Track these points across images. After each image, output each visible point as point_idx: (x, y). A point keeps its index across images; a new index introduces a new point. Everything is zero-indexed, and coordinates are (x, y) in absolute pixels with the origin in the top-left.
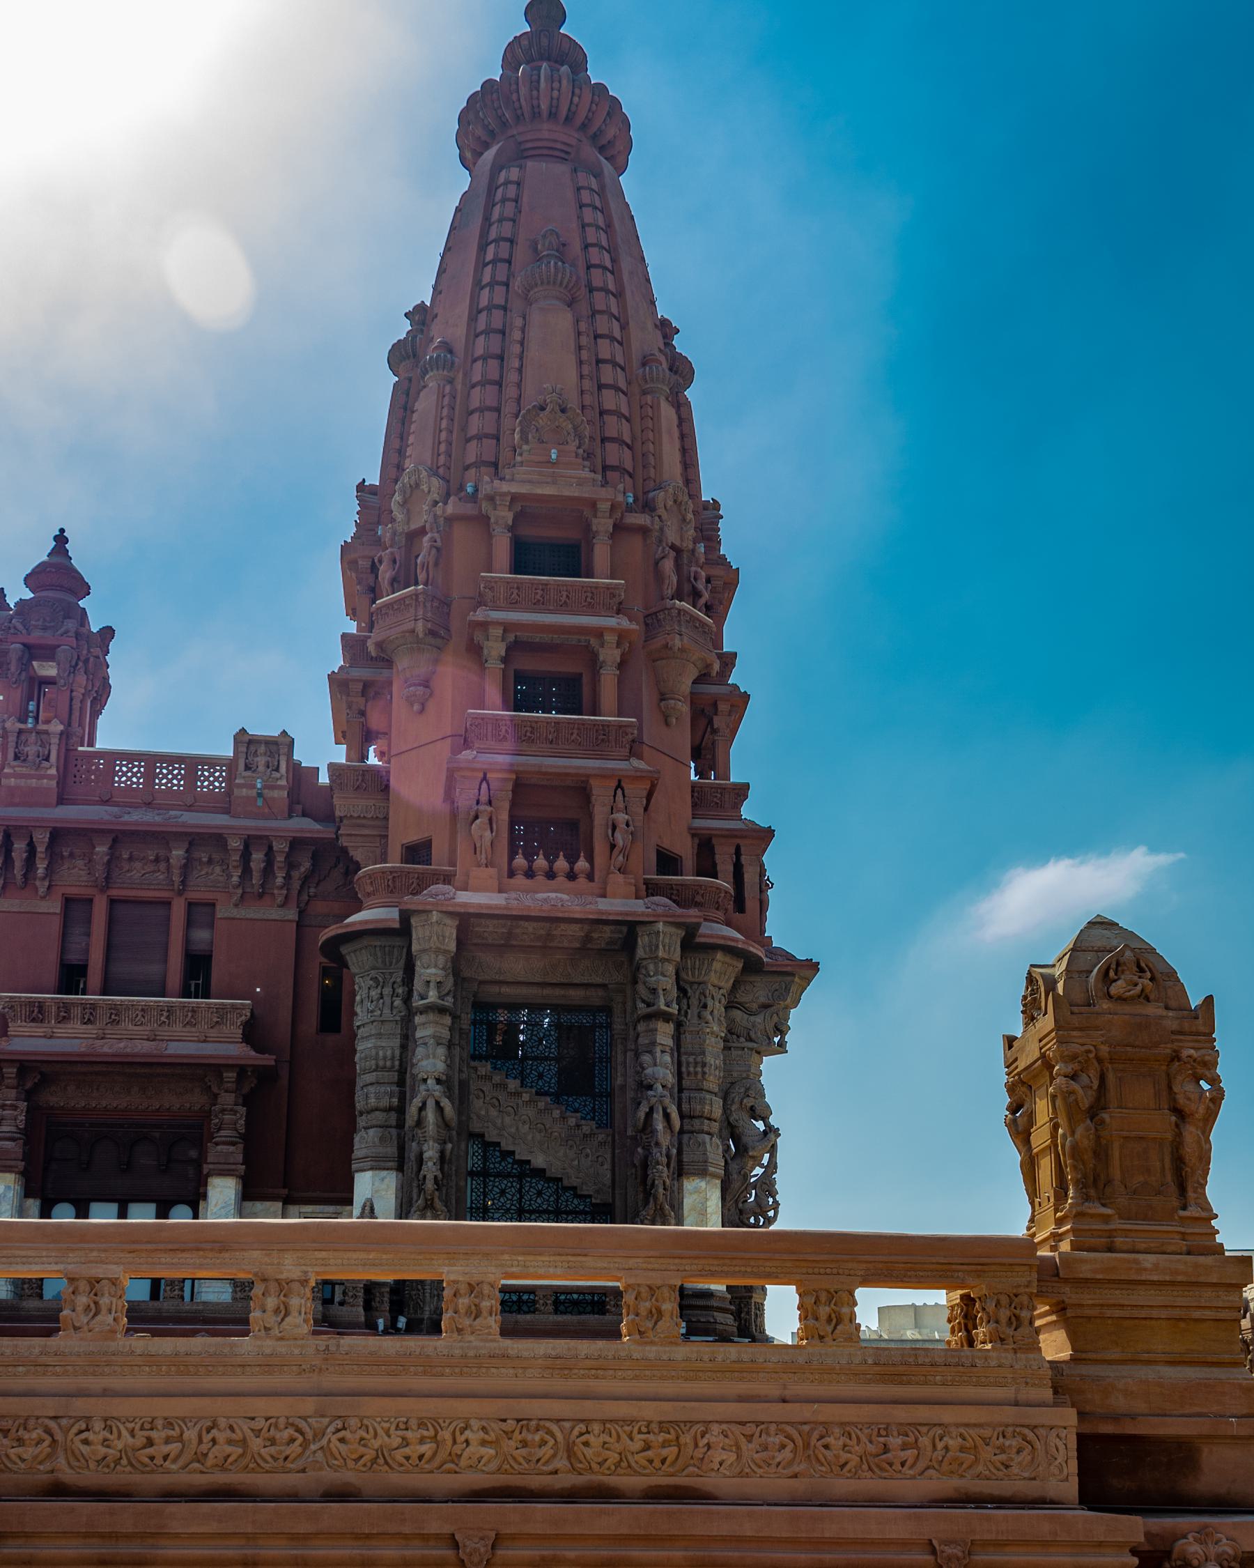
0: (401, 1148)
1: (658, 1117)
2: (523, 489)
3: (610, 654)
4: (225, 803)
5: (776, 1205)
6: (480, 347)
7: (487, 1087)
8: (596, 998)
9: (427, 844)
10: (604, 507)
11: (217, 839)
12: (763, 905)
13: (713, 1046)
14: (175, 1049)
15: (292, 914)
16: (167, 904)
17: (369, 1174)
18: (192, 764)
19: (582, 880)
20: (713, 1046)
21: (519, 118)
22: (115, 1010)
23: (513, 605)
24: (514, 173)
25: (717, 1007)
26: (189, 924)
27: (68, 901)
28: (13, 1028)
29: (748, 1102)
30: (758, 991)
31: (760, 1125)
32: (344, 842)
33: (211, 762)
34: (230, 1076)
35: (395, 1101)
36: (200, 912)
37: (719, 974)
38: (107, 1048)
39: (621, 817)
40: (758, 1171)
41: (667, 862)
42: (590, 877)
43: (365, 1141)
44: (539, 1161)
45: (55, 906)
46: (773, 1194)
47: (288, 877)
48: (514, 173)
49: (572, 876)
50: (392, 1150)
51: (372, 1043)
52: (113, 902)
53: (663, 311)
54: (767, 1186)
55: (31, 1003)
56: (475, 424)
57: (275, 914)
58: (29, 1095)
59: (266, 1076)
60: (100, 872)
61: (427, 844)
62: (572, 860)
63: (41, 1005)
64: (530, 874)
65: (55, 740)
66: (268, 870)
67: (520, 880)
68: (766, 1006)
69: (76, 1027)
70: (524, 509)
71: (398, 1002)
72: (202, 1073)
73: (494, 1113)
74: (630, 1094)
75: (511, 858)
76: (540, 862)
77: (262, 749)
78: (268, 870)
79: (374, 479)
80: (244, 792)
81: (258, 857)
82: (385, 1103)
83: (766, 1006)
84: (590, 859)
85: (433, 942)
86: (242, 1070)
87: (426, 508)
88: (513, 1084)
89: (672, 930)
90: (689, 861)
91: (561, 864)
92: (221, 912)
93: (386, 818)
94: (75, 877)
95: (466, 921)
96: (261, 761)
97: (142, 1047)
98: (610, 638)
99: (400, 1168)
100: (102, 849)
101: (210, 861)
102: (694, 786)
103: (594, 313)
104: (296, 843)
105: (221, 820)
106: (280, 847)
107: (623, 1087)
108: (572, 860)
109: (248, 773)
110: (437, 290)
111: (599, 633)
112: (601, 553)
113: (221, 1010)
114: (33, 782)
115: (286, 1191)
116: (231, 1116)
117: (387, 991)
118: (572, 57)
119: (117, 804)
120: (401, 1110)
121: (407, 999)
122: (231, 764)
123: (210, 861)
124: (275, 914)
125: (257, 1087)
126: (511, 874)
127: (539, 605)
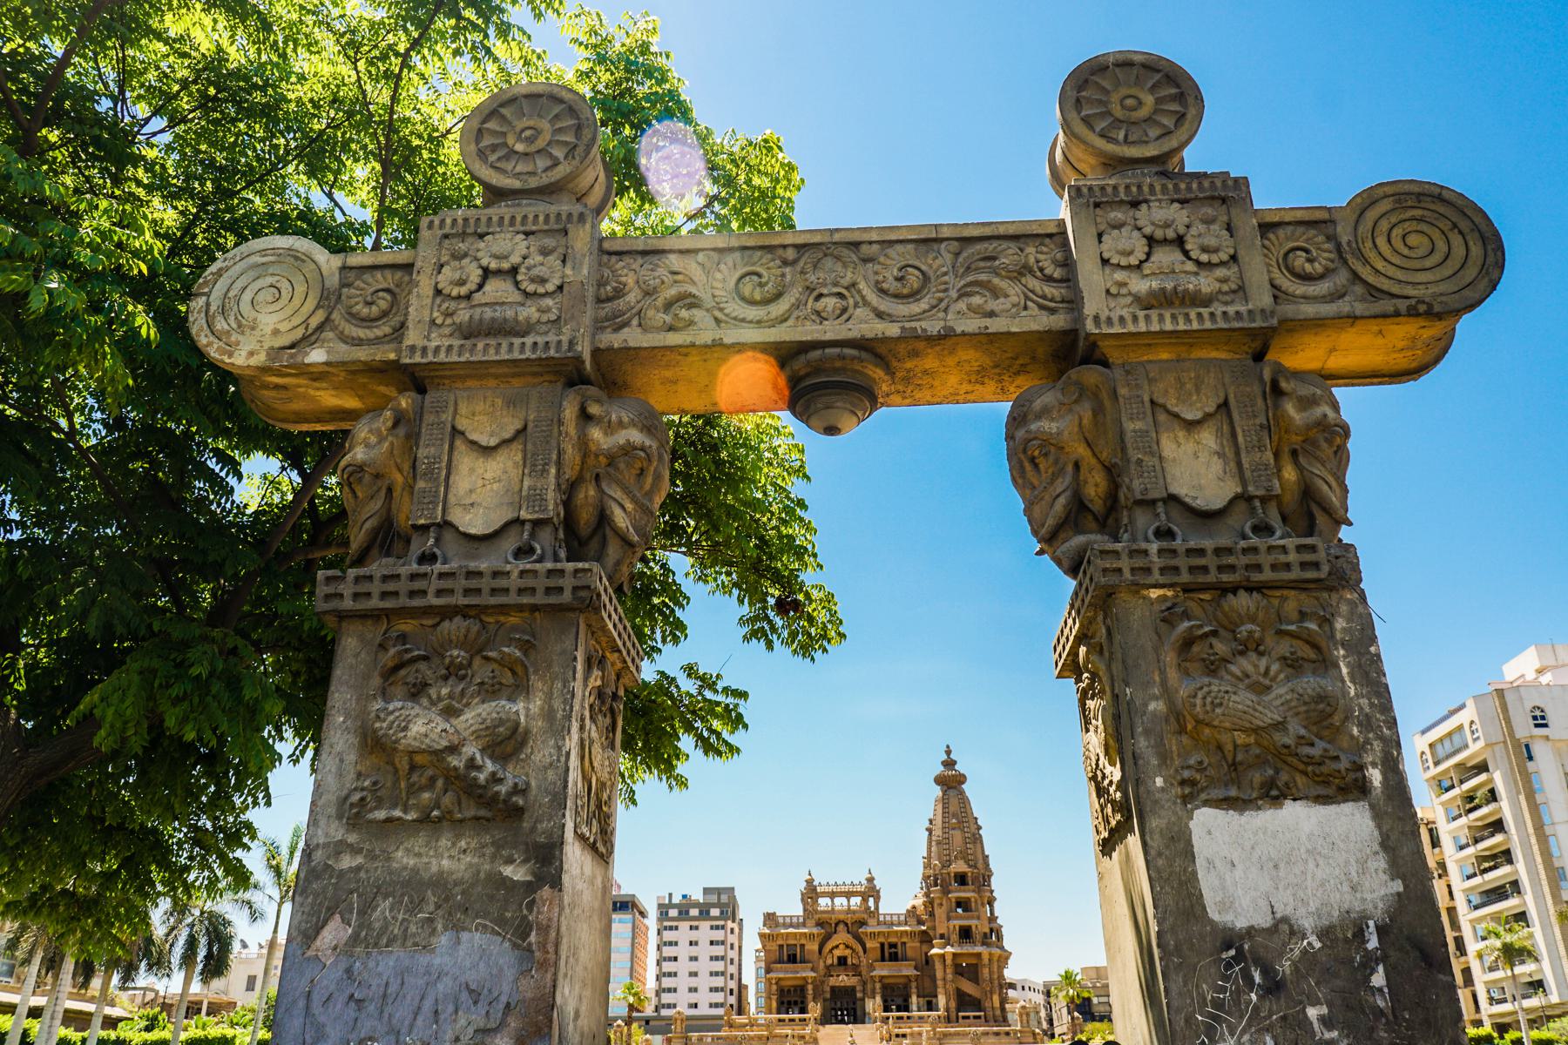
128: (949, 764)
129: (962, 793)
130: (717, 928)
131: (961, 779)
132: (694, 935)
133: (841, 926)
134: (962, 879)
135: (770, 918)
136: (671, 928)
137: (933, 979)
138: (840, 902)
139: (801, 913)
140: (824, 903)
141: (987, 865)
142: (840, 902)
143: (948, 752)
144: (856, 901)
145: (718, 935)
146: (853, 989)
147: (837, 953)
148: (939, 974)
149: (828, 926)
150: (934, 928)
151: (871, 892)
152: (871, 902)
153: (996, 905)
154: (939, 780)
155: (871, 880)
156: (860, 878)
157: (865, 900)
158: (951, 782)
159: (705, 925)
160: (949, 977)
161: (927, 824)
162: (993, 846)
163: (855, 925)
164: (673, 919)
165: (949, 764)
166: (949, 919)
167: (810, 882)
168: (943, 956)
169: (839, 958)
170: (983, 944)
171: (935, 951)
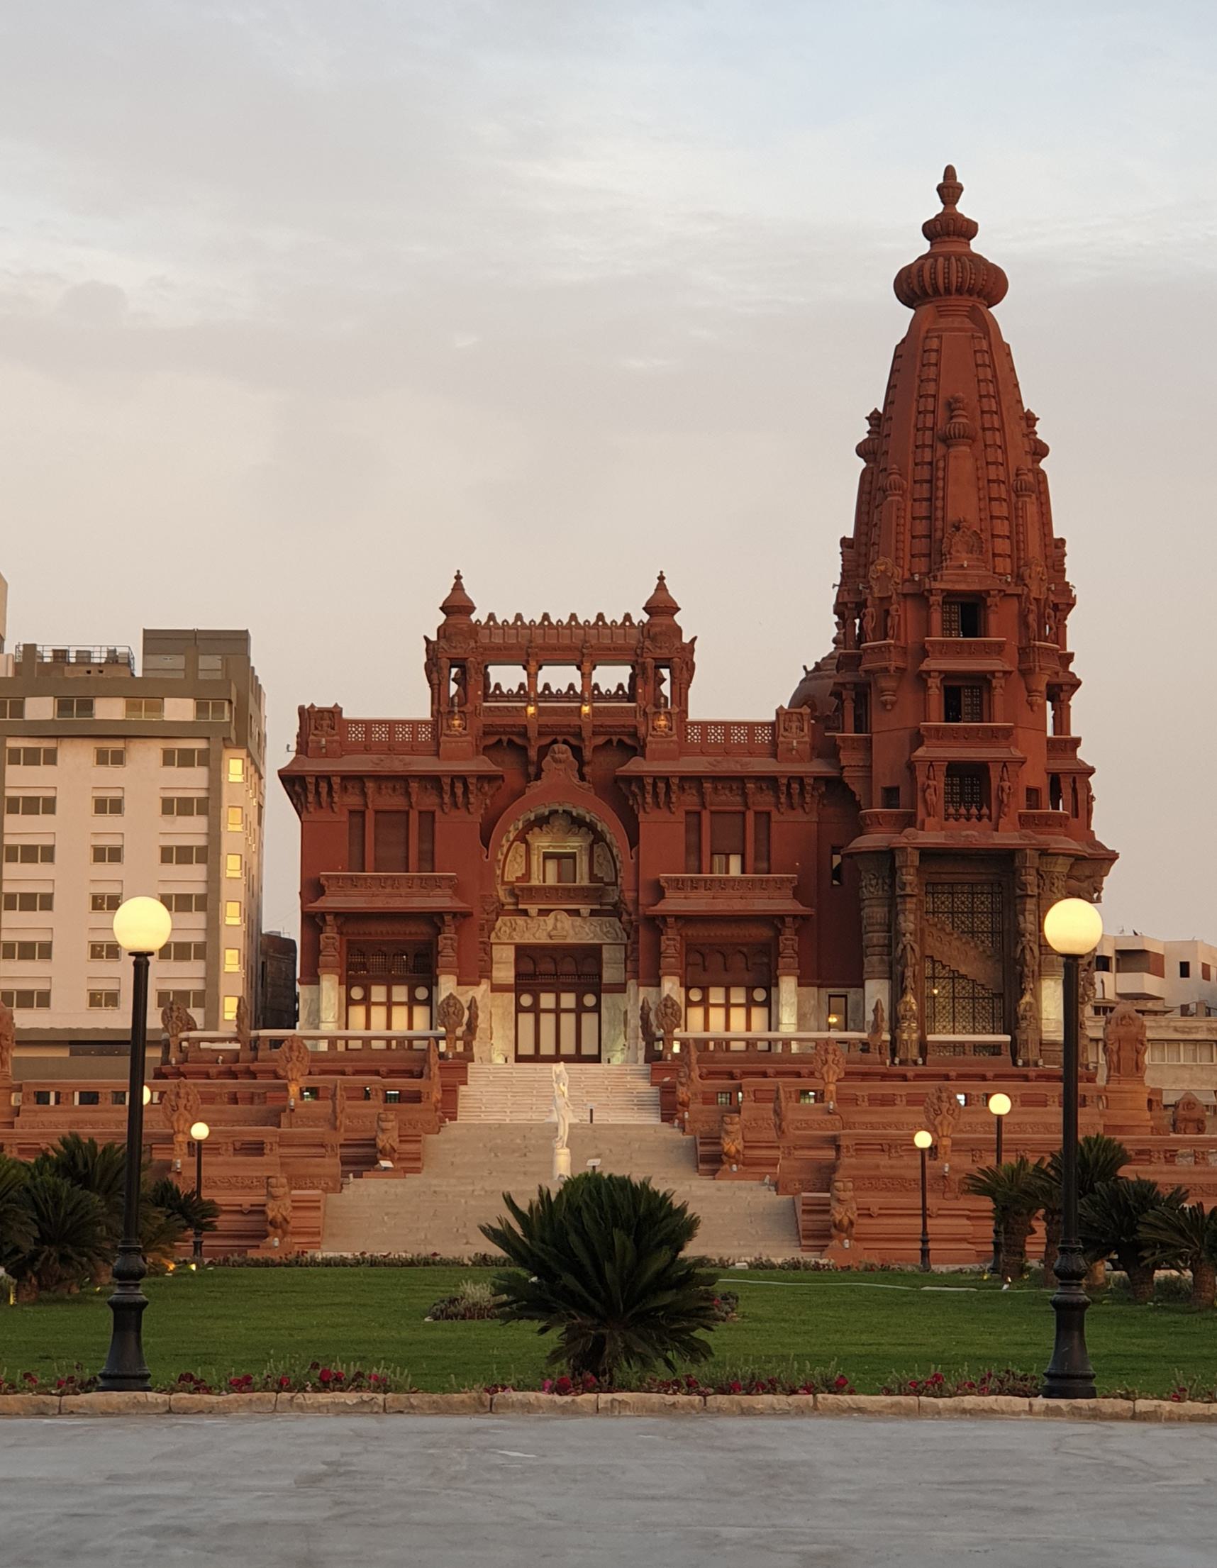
1: (1028, 952)
2: (949, 587)
12: (1089, 812)
18: (751, 726)
19: (985, 820)
39: (1006, 784)
44: (963, 971)
49: (980, 818)
53: (1027, 405)
59: (805, 918)
72: (774, 921)
73: (938, 944)
79: (850, 535)
82: (881, 942)
84: (989, 808)
86: (795, 917)
89: (1033, 852)
90: (1045, 796)
91: (974, 811)
92: (775, 817)
99: (890, 978)
102: (1049, 740)
109: (786, 734)
114: (666, 746)
115: (819, 982)
116: (789, 941)
118: (968, 229)
120: (890, 946)
121: (892, 886)
122: (772, 724)
128: (949, 230)
129: (989, 330)
130: (186, 759)
131: (991, 284)
132: (110, 779)
135: (317, 723)
136: (32, 758)
137: (856, 927)
138: (560, 677)
141: (1058, 569)
142: (560, 677)
143: (949, 189)
144: (611, 677)
145: (192, 781)
146: (593, 953)
148: (874, 912)
151: (657, 644)
153: (1076, 701)
154: (910, 286)
155: (661, 606)
156: (625, 603)
157: (643, 676)
158: (950, 283)
159: (145, 756)
161: (862, 431)
162: (1079, 507)
164: (38, 730)
165: (949, 230)
166: (918, 739)
167: (457, 606)
168: (888, 857)
170: (1025, 821)
171: (871, 841)
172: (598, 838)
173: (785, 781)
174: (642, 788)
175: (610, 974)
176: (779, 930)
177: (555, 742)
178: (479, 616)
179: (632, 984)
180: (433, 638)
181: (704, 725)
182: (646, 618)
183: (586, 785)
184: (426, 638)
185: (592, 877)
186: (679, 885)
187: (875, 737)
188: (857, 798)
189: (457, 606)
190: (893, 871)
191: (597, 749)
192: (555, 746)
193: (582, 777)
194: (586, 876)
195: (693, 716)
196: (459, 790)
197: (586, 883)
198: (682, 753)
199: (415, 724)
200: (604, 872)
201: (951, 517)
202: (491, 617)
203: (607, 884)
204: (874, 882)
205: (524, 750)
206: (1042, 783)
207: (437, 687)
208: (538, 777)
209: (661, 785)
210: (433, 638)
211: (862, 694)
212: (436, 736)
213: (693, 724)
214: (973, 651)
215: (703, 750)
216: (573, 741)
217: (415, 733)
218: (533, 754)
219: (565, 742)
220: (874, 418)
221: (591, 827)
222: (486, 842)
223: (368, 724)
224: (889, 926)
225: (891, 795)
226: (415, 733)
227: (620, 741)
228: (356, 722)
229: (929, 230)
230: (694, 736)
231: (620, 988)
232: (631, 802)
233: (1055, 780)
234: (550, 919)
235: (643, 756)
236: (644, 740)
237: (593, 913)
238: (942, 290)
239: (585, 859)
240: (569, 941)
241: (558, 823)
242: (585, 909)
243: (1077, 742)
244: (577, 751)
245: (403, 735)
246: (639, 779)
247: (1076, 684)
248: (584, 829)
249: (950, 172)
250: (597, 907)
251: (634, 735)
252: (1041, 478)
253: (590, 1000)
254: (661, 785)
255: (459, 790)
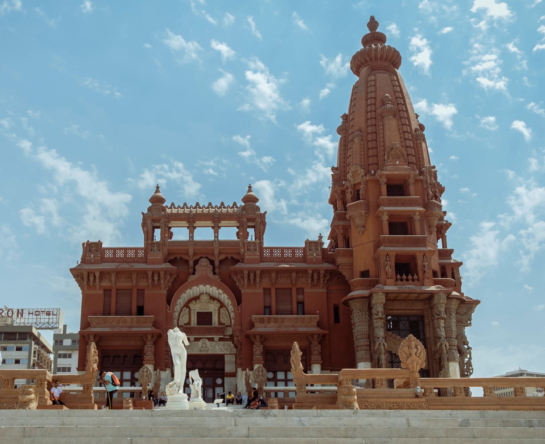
0: (371, 356)
1: (444, 346)
3: (417, 217)
4: (304, 259)
5: (472, 369)
6: (370, 130)
7: (391, 338)
8: (419, 313)
9: (368, 272)
10: (412, 176)
11: (304, 271)
13: (454, 325)
14: (300, 329)
15: (325, 290)
16: (291, 289)
17: (363, 363)
18: (293, 249)
19: (416, 281)
20: (454, 325)
21: (371, 60)
22: (283, 319)
23: (389, 205)
24: (373, 78)
25: (454, 314)
26: (297, 294)
27: (264, 289)
28: (256, 325)
29: (463, 340)
30: (464, 310)
31: (466, 346)
32: (340, 270)
33: (299, 249)
34: (316, 336)
35: (368, 343)
36: (300, 291)
37: (454, 305)
38: (282, 330)
39: (426, 263)
40: (467, 359)
41: (435, 274)
42: (418, 280)
43: (360, 354)
45: (261, 291)
46: (471, 366)
47: (324, 280)
48: (373, 78)
49: (413, 280)
50: (369, 356)
51: (360, 327)
52: (276, 289)
54: (469, 364)
55: (261, 318)
56: (371, 152)
57: (320, 290)
58: (262, 343)
59: (324, 336)
60: (274, 281)
61: (368, 272)
62: (413, 276)
63: (263, 319)
64: (402, 280)
65: (257, 245)
66: (319, 279)
67: (399, 282)
68: (466, 313)
69: (272, 324)
70: (389, 178)
71: (367, 316)
73: (393, 345)
74: (432, 339)
75: (396, 275)
76: (404, 277)
77: (313, 244)
78: (319, 279)
80: (310, 257)
81: (315, 275)
82: (366, 343)
83: (466, 313)
84: (417, 275)
85: (379, 300)
86: (319, 335)
87: (360, 177)
88: (398, 337)
89: (444, 294)
90: (439, 274)
91: (410, 277)
92: (306, 291)
93: (352, 264)
94: (266, 283)
95: (387, 294)
96: (313, 248)
97: (291, 329)
98: (417, 213)
99: (371, 361)
100: (274, 275)
101: (302, 277)
103: (401, 118)
104: (326, 271)
105: (303, 265)
106: (322, 272)
107: (430, 337)
108: (413, 276)
109: (310, 252)
110: (350, 110)
111: (414, 212)
112: (412, 189)
113: (311, 318)
114: (253, 257)
115: (331, 368)
117: (364, 313)
119: (275, 262)
120: (370, 346)
121: (370, 315)
122: (304, 249)
123: (302, 277)
124: (320, 290)
125: (322, 339)
126: (397, 280)
127: (396, 205)
133: (204, 262)
134: (397, 188)
138: (204, 234)
139: (140, 243)
140: (180, 234)
143: (373, 24)
146: (220, 358)
147: (196, 307)
149: (182, 263)
150: (351, 265)
151: (249, 214)
152: (251, 232)
155: (251, 200)
156: (234, 198)
157: (242, 234)
158: (377, 60)
160: (380, 333)
161: (339, 122)
163: (226, 264)
166: (378, 245)
167: (157, 200)
169: (200, 315)
172: (222, 305)
173: (310, 272)
174: (243, 278)
175: (229, 368)
176: (311, 342)
177: (202, 258)
178: (167, 204)
179: (239, 370)
180: (146, 212)
181: (271, 249)
182: (243, 204)
183: (217, 276)
184: (143, 213)
185: (220, 323)
186: (262, 321)
187: (354, 249)
188: (346, 279)
189: (157, 200)
190: (370, 308)
191: (221, 262)
192: (202, 259)
193: (214, 274)
194: (217, 323)
195: (265, 245)
196: (156, 278)
197: (217, 325)
198: (261, 261)
199: (136, 249)
200: (225, 320)
201: (387, 144)
202: (173, 204)
203: (227, 326)
204: (360, 314)
205: (187, 262)
206: (437, 268)
207: (149, 236)
208: (194, 273)
209: (252, 275)
210: (146, 212)
211: (346, 229)
212: (146, 254)
213: (266, 248)
214: (403, 205)
215: (272, 259)
216: (211, 258)
217: (136, 253)
218: (191, 263)
219: (207, 258)
220: (345, 118)
221: (219, 301)
222: (169, 302)
223: (114, 250)
224: (369, 335)
225: (365, 274)
226: (136, 253)
227: (232, 258)
228: (109, 249)
229: (366, 41)
230: (267, 254)
231: (234, 375)
232: (237, 284)
233: (443, 268)
234: (200, 343)
235: (243, 262)
236: (244, 255)
237: (220, 340)
238: (374, 59)
239: (217, 315)
240: (209, 353)
241: (204, 298)
242: (216, 338)
243: (451, 251)
244: (212, 262)
245: (131, 254)
246: (242, 271)
247: (448, 225)
248: (216, 301)
249: (372, 18)
250: (222, 336)
251: (239, 254)
252: (423, 135)
253: (219, 381)
254: (252, 275)
255: (156, 278)
